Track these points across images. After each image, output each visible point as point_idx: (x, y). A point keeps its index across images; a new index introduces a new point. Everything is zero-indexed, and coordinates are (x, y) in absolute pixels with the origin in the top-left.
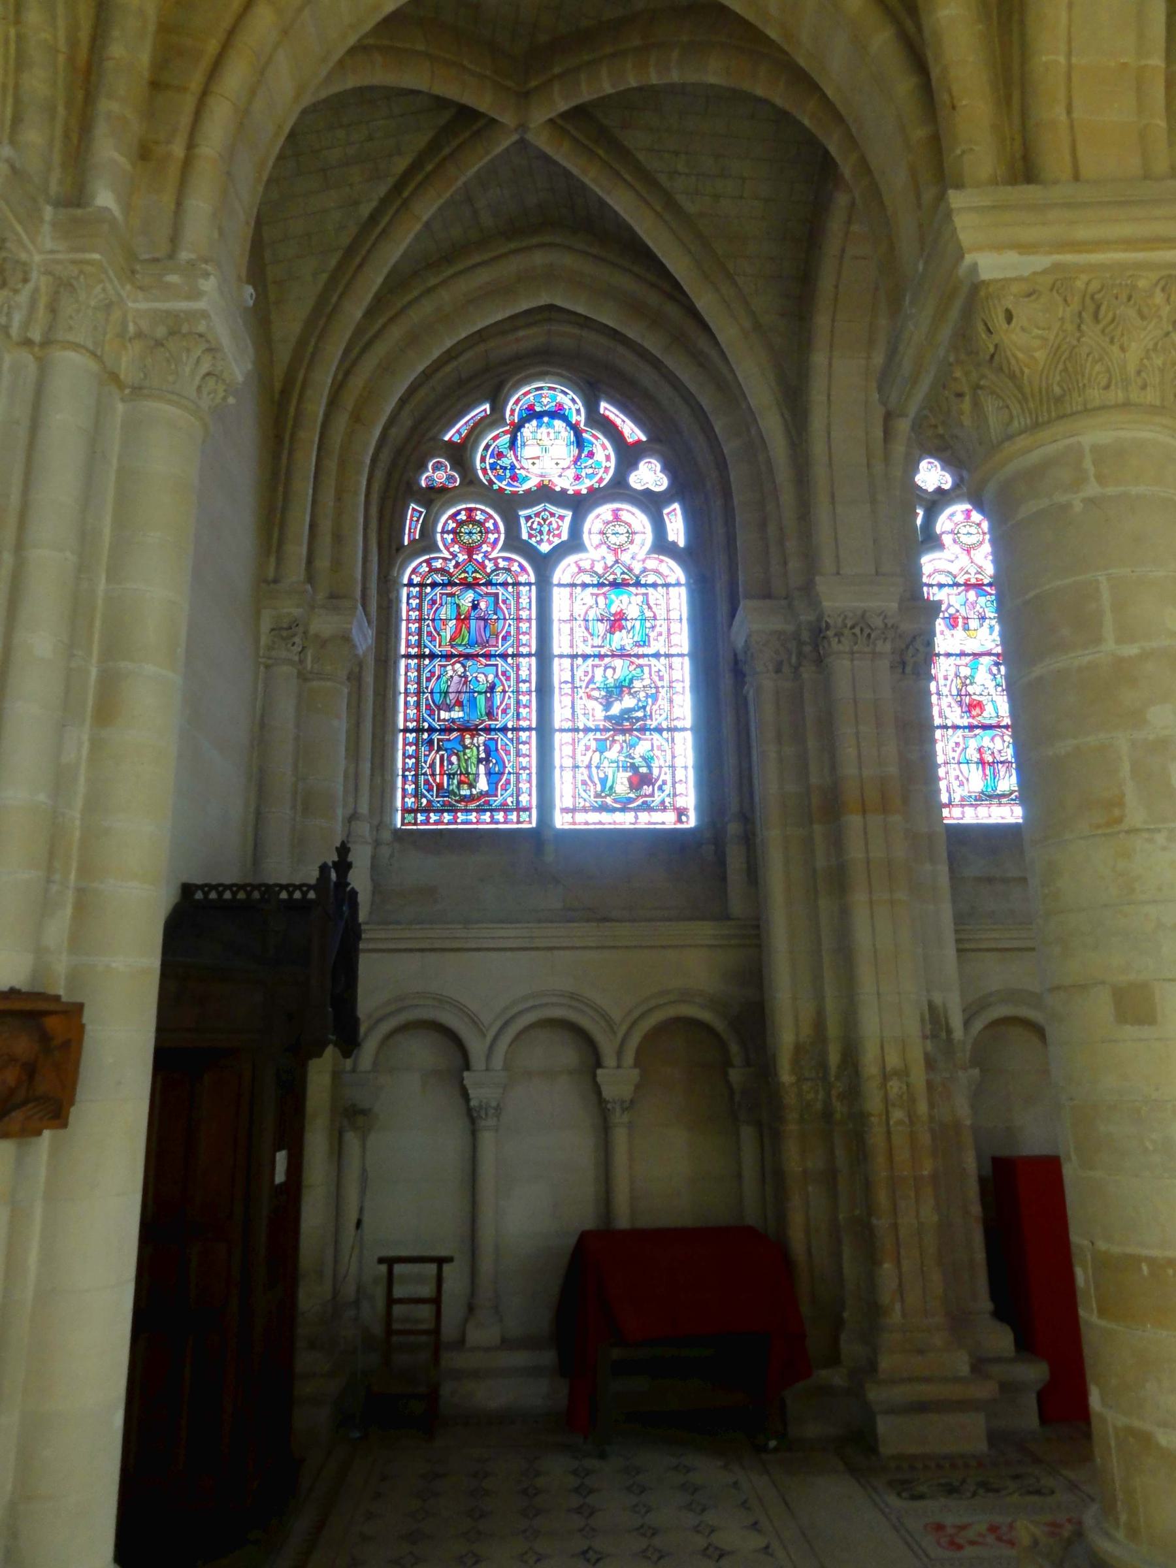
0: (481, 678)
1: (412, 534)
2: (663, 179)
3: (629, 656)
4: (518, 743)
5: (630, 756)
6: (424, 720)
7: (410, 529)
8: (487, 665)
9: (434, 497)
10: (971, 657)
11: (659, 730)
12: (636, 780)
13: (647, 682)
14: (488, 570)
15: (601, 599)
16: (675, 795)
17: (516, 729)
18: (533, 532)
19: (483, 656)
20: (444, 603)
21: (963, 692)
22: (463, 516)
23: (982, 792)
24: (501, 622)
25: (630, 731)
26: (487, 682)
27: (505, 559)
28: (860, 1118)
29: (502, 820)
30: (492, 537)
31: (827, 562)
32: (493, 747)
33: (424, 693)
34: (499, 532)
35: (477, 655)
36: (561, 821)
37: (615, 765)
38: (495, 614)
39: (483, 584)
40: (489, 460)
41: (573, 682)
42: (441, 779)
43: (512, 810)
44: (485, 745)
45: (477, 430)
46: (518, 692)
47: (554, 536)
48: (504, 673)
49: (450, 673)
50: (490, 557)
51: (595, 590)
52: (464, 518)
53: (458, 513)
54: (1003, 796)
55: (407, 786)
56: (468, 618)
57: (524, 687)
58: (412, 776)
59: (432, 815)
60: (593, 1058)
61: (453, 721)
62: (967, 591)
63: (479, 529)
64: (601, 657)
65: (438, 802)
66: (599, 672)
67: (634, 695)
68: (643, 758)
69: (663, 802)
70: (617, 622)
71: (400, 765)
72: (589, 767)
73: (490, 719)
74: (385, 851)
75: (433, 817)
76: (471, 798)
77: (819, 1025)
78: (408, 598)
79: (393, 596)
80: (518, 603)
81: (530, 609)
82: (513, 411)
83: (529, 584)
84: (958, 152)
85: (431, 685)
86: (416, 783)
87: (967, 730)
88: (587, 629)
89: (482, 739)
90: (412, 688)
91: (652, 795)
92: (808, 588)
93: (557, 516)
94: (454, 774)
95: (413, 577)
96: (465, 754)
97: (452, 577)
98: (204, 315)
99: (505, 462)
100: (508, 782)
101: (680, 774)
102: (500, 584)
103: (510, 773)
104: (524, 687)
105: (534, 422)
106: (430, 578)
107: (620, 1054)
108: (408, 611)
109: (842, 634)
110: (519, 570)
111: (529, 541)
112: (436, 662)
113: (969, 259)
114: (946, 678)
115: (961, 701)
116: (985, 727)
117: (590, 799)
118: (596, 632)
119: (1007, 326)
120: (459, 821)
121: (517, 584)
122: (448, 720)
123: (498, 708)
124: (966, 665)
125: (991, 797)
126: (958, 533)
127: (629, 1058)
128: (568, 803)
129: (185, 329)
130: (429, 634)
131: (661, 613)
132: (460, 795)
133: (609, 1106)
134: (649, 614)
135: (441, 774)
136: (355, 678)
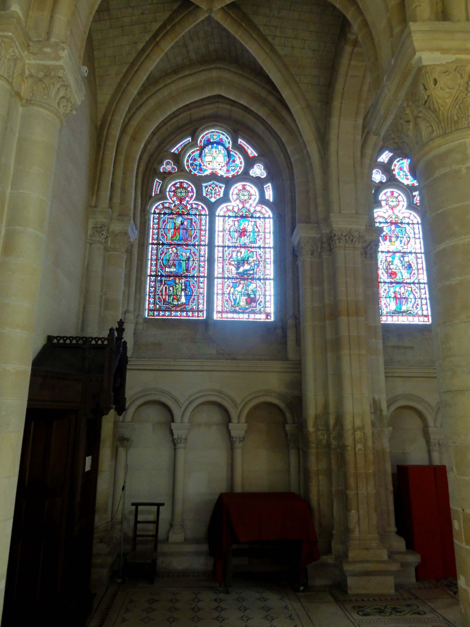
0: (184, 254)
1: (156, 192)
2: (270, 39)
3: (248, 247)
4: (199, 283)
5: (247, 290)
6: (159, 272)
7: (155, 189)
8: (186, 249)
9: (166, 176)
10: (392, 253)
11: (259, 279)
12: (249, 300)
13: (255, 259)
14: (188, 209)
15: (236, 223)
16: (265, 307)
18: (208, 193)
19: (185, 245)
20: (169, 222)
21: (388, 268)
22: (178, 185)
23: (395, 310)
24: (193, 231)
25: (247, 279)
26: (186, 256)
27: (195, 204)
28: (343, 448)
29: (191, 315)
31: (335, 207)
32: (188, 284)
33: (159, 260)
34: (193, 193)
35: (182, 245)
36: (216, 317)
37: (240, 293)
38: (191, 227)
39: (186, 214)
40: (190, 162)
41: (223, 257)
42: (166, 297)
43: (195, 311)
44: (185, 283)
45: (185, 148)
47: (217, 195)
48: (194, 253)
49: (171, 252)
50: (189, 203)
51: (234, 219)
52: (179, 186)
53: (176, 184)
54: (404, 312)
55: (150, 300)
56: (179, 228)
57: (202, 259)
58: (153, 295)
59: (161, 312)
61: (171, 272)
62: (391, 225)
63: (185, 191)
64: (236, 247)
65: (164, 307)
66: (234, 254)
67: (249, 264)
68: (252, 291)
69: (260, 310)
70: (243, 233)
71: (148, 290)
72: (229, 294)
73: (187, 272)
74: (140, 327)
75: (161, 313)
76: (178, 306)
77: (326, 406)
78: (154, 219)
79: (147, 217)
80: (201, 223)
81: (206, 226)
82: (201, 141)
83: (206, 215)
84: (414, 6)
85: (162, 256)
86: (154, 298)
87: (389, 284)
88: (230, 235)
89: (183, 281)
90: (154, 257)
91: (256, 307)
92: (327, 219)
93: (218, 186)
94: (171, 295)
95: (156, 210)
96: (176, 287)
97: (172, 211)
98: (62, 68)
99: (197, 163)
100: (194, 299)
101: (268, 298)
102: (193, 215)
103: (195, 295)
104: (202, 259)
105: (210, 146)
106: (163, 211)
107: (239, 417)
108: (153, 225)
109: (341, 239)
110: (201, 209)
111: (206, 197)
112: (165, 247)
113: (418, 55)
114: (381, 262)
115: (387, 272)
116: (397, 283)
117: (228, 307)
118: (234, 237)
119: (434, 86)
120: (172, 315)
121: (200, 215)
122: (169, 272)
123: (191, 267)
124: (390, 257)
125: (399, 312)
126: (388, 201)
127: (243, 419)
128: (220, 309)
129: (53, 74)
130: (162, 235)
131: (261, 229)
132: (173, 304)
133: (234, 439)
134: (257, 230)
135: (165, 295)
136: (129, 252)
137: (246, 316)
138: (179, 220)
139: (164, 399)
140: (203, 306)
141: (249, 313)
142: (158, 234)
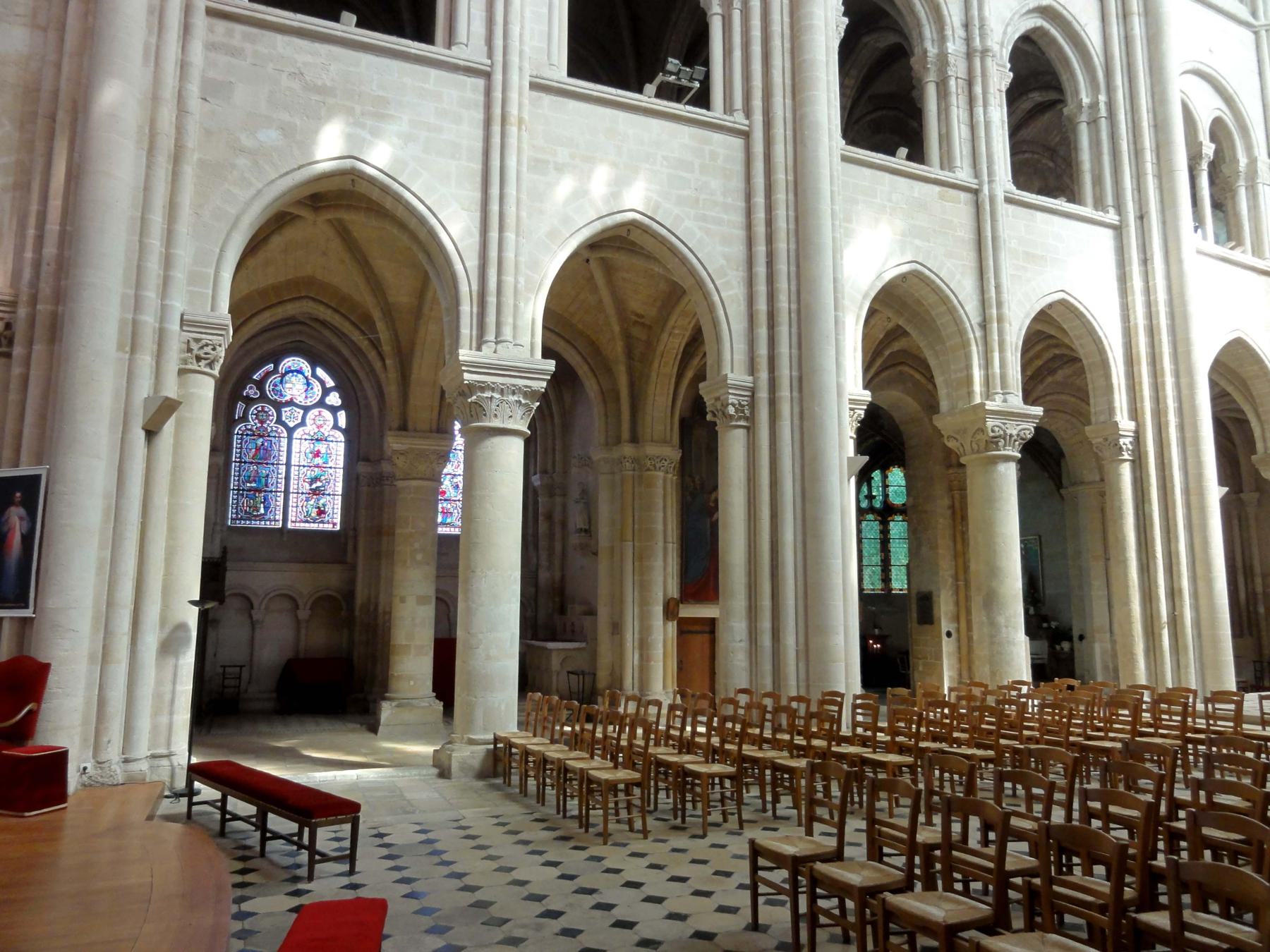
9: (249, 401)
11: (329, 495)
15: (312, 446)
17: (276, 492)
25: (318, 494)
30: (271, 418)
36: (290, 526)
45: (268, 374)
46: (277, 478)
57: (280, 476)
60: (297, 607)
64: (310, 467)
67: (321, 482)
70: (317, 454)
75: (243, 522)
76: (257, 516)
99: (278, 388)
104: (280, 476)
105: (291, 374)
112: (247, 465)
116: (445, 500)
121: (279, 437)
127: (308, 607)
128: (294, 519)
131: (334, 452)
137: (316, 525)
138: (260, 441)
139: (246, 593)
140: (280, 517)
142: (240, 453)
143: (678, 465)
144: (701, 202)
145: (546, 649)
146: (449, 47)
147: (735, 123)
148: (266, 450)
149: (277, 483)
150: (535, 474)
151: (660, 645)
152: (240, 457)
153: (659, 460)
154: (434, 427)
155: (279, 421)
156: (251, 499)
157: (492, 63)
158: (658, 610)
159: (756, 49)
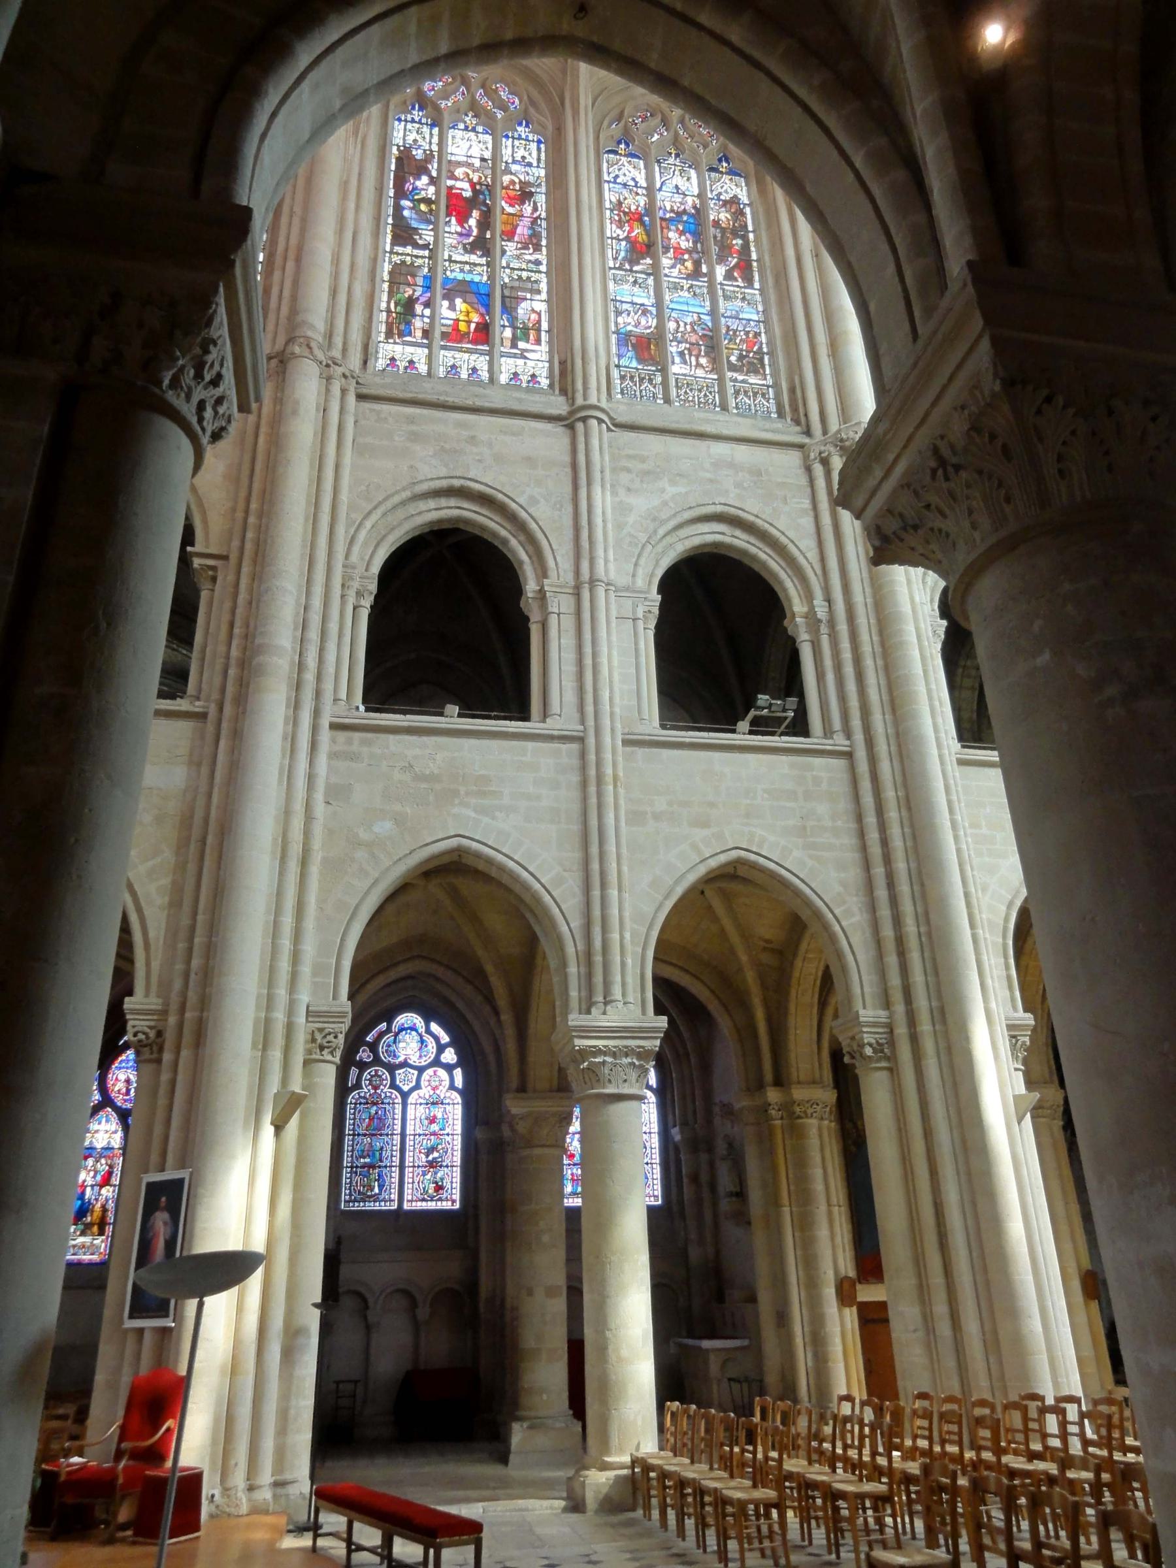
9: (363, 1066)
15: (427, 1110)
22: (373, 1073)
36: (406, 1206)
45: (381, 1035)
46: (392, 1150)
57: (394, 1148)
66: (425, 1142)
67: (438, 1151)
70: (433, 1120)
75: (356, 1204)
86: (350, 1189)
104: (394, 1148)
112: (361, 1137)
121: (394, 1103)
128: (410, 1198)
138: (373, 1110)
139: (362, 1290)
140: (394, 1196)
141: (437, 1201)
143: (834, 1109)
144: (808, 829)
145: (700, 1348)
146: (544, 721)
147: (835, 745)
148: (380, 1119)
149: (392, 1156)
150: (675, 1126)
151: (838, 1340)
152: (354, 1130)
153: (809, 1105)
154: (555, 1083)
155: (393, 1086)
156: (365, 1176)
157: (585, 729)
158: (829, 1292)
159: (849, 670)
